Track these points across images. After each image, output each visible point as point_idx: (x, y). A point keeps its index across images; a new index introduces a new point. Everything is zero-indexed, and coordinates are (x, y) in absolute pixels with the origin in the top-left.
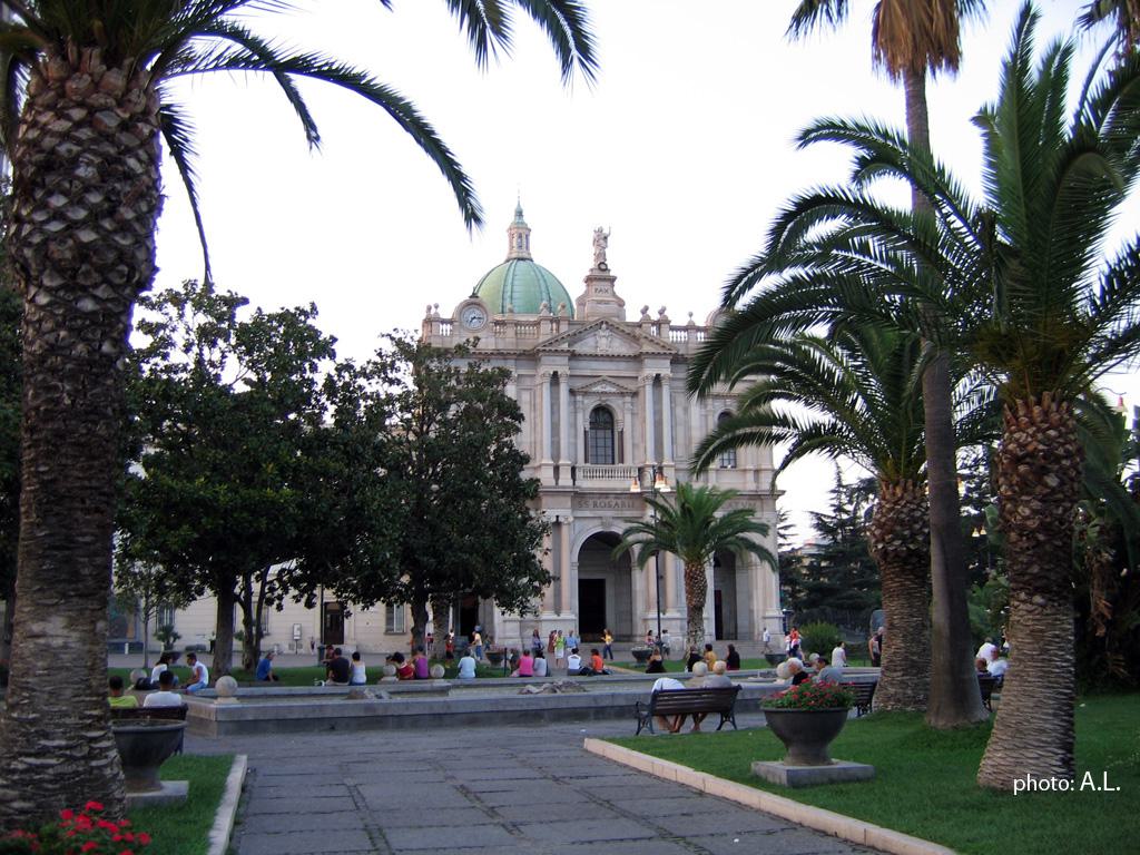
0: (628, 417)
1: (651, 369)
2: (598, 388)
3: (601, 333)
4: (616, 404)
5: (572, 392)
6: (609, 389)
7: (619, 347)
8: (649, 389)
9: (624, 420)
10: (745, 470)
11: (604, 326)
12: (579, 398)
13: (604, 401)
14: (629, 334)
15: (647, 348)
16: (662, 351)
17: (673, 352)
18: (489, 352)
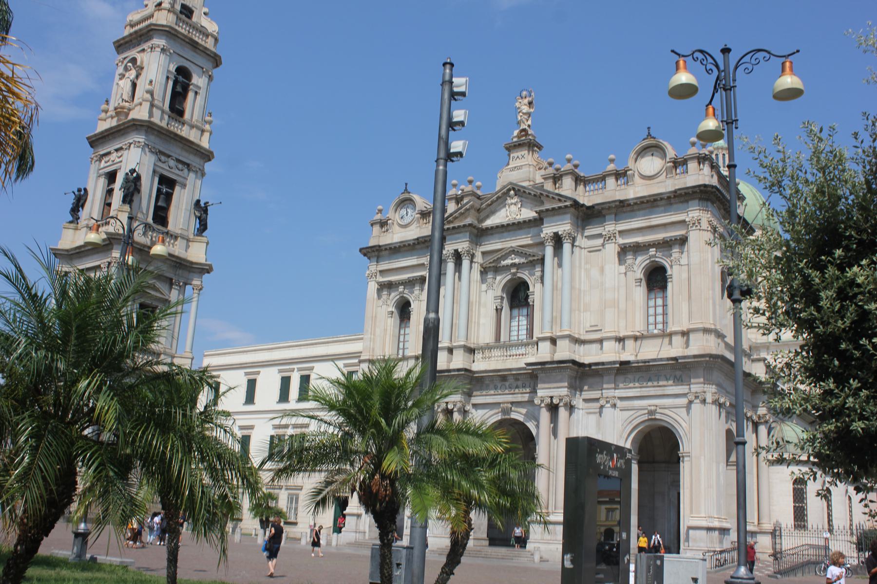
0: (538, 286)
1: (548, 230)
2: (508, 262)
3: (509, 201)
4: (524, 275)
5: (484, 272)
6: (517, 261)
7: (528, 214)
8: (549, 251)
9: (536, 291)
10: (670, 335)
11: (512, 192)
12: (490, 276)
13: (514, 274)
14: (535, 195)
15: (548, 206)
16: (555, 206)
17: (568, 203)
18: (411, 243)
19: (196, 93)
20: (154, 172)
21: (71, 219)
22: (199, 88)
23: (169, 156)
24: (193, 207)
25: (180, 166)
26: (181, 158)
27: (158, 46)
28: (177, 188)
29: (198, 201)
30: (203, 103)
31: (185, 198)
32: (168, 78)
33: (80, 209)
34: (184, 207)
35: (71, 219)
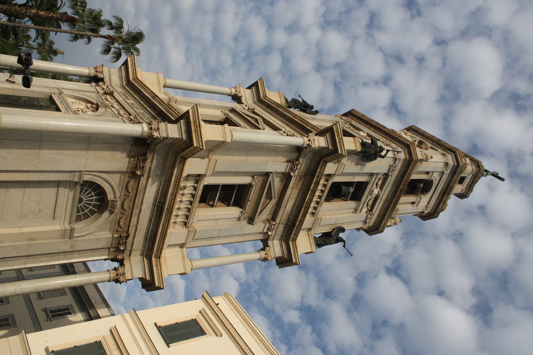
19: (413, 203)
20: (372, 175)
21: (289, 100)
22: (417, 206)
23: (381, 188)
24: (338, 226)
25: (370, 203)
26: (379, 201)
27: (447, 160)
28: (352, 204)
29: (343, 230)
30: (408, 212)
31: (343, 215)
32: (427, 173)
33: (299, 110)
34: (339, 216)
35: (289, 100)
